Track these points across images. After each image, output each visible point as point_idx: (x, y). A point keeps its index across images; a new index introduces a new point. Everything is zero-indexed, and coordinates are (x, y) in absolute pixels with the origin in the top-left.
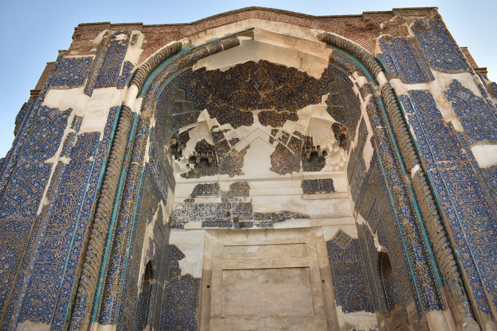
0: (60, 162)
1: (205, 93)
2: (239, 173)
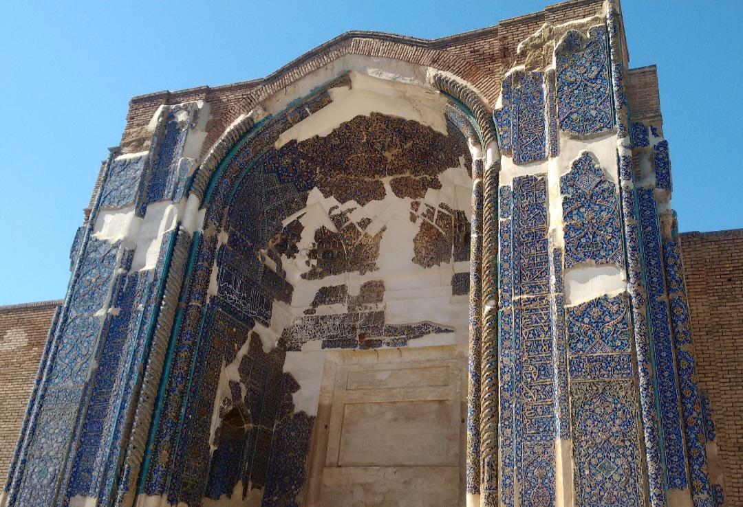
1: (308, 168)
2: (372, 267)
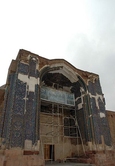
0: (27, 100)
